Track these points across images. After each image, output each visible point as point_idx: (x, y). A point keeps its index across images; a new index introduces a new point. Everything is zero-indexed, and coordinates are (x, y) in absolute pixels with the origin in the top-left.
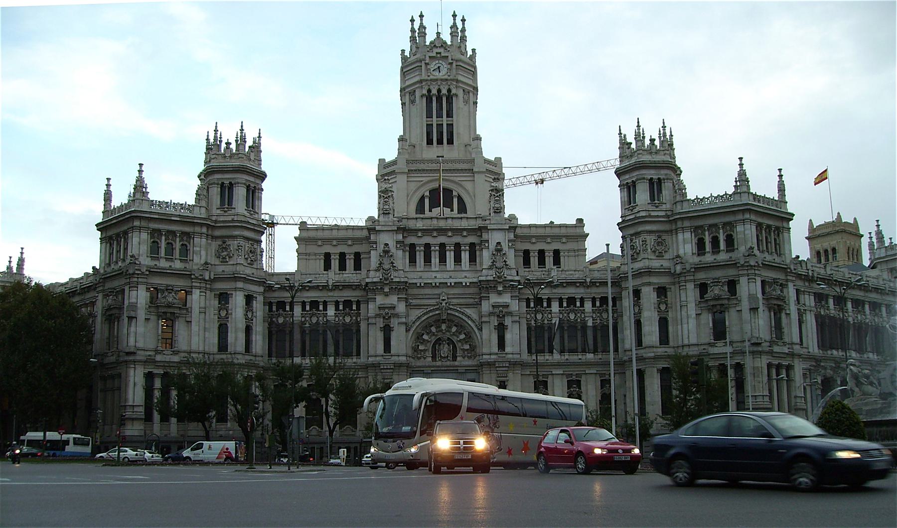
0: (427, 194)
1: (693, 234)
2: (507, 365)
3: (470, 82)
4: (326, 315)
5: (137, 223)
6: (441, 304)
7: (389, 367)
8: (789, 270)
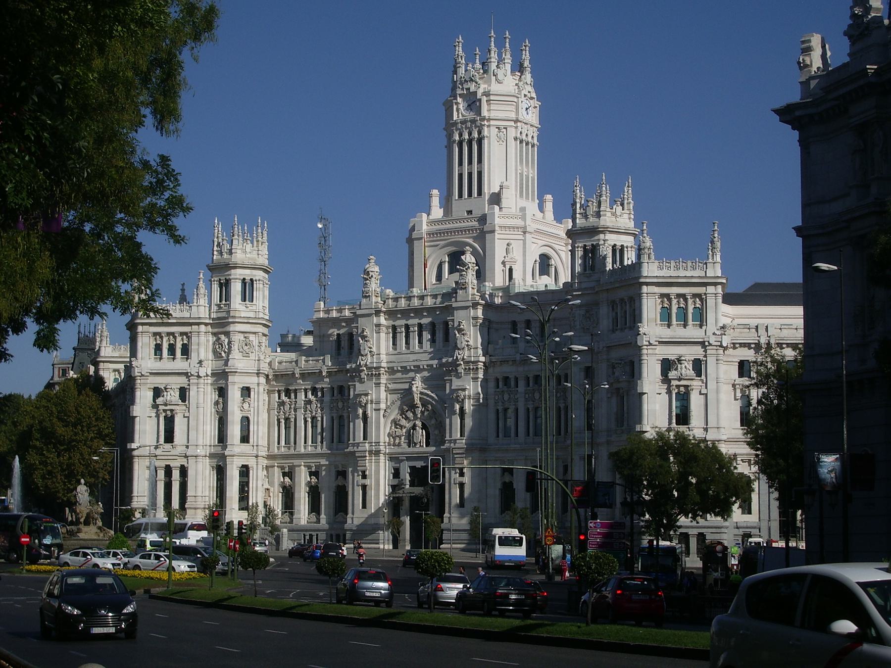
1: (611, 309)
3: (513, 116)
5: (140, 328)
7: (363, 455)
8: (707, 344)
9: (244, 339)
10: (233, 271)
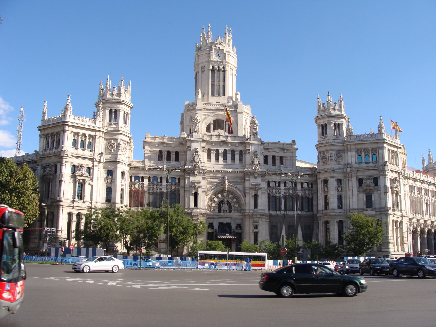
0: (212, 122)
1: (356, 153)
2: (259, 216)
4: (161, 185)
5: (67, 128)
6: (225, 182)
7: (197, 215)
8: (401, 174)
9: (124, 144)
10: (121, 106)
